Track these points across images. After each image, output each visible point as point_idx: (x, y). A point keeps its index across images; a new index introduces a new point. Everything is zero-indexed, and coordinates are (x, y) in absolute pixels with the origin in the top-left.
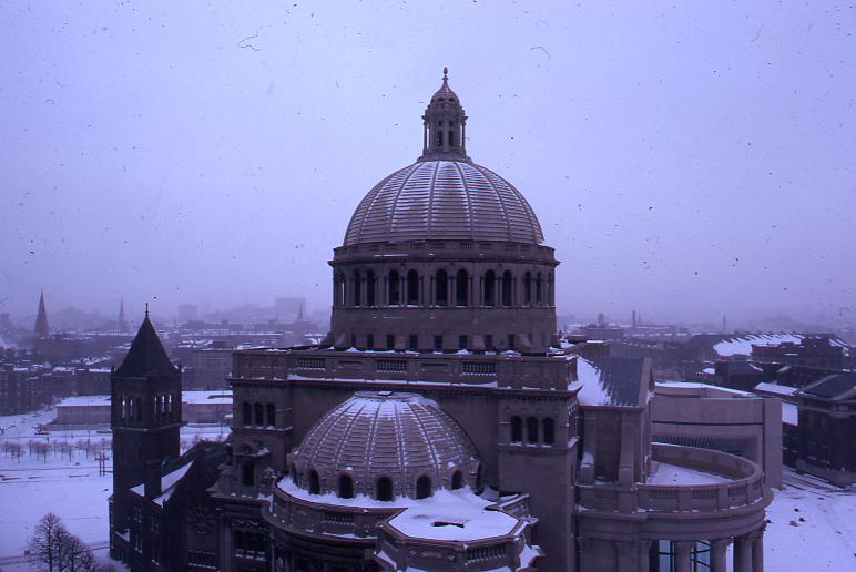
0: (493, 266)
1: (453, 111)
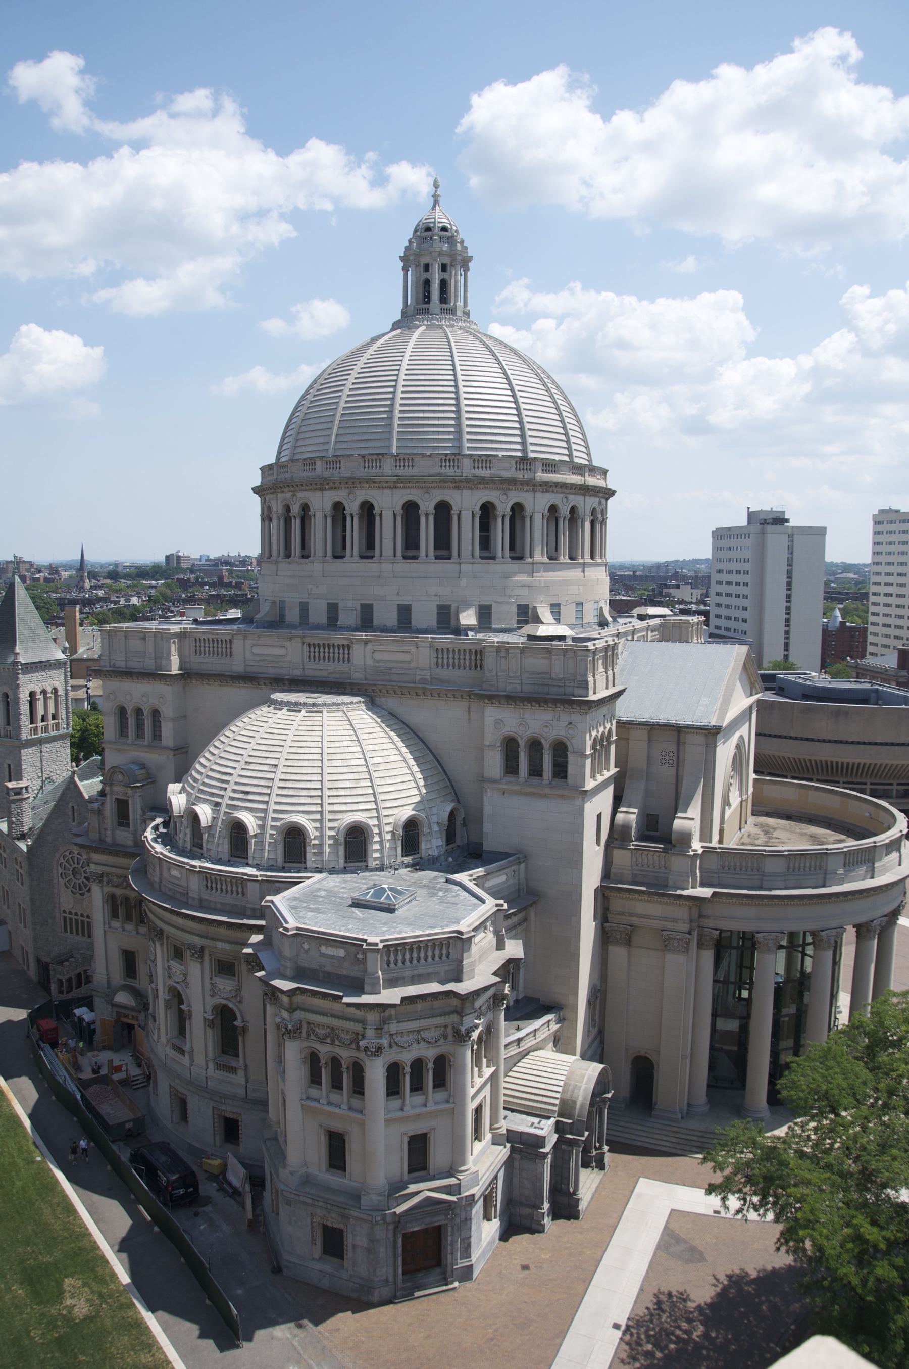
0: (492, 495)
1: (445, 247)
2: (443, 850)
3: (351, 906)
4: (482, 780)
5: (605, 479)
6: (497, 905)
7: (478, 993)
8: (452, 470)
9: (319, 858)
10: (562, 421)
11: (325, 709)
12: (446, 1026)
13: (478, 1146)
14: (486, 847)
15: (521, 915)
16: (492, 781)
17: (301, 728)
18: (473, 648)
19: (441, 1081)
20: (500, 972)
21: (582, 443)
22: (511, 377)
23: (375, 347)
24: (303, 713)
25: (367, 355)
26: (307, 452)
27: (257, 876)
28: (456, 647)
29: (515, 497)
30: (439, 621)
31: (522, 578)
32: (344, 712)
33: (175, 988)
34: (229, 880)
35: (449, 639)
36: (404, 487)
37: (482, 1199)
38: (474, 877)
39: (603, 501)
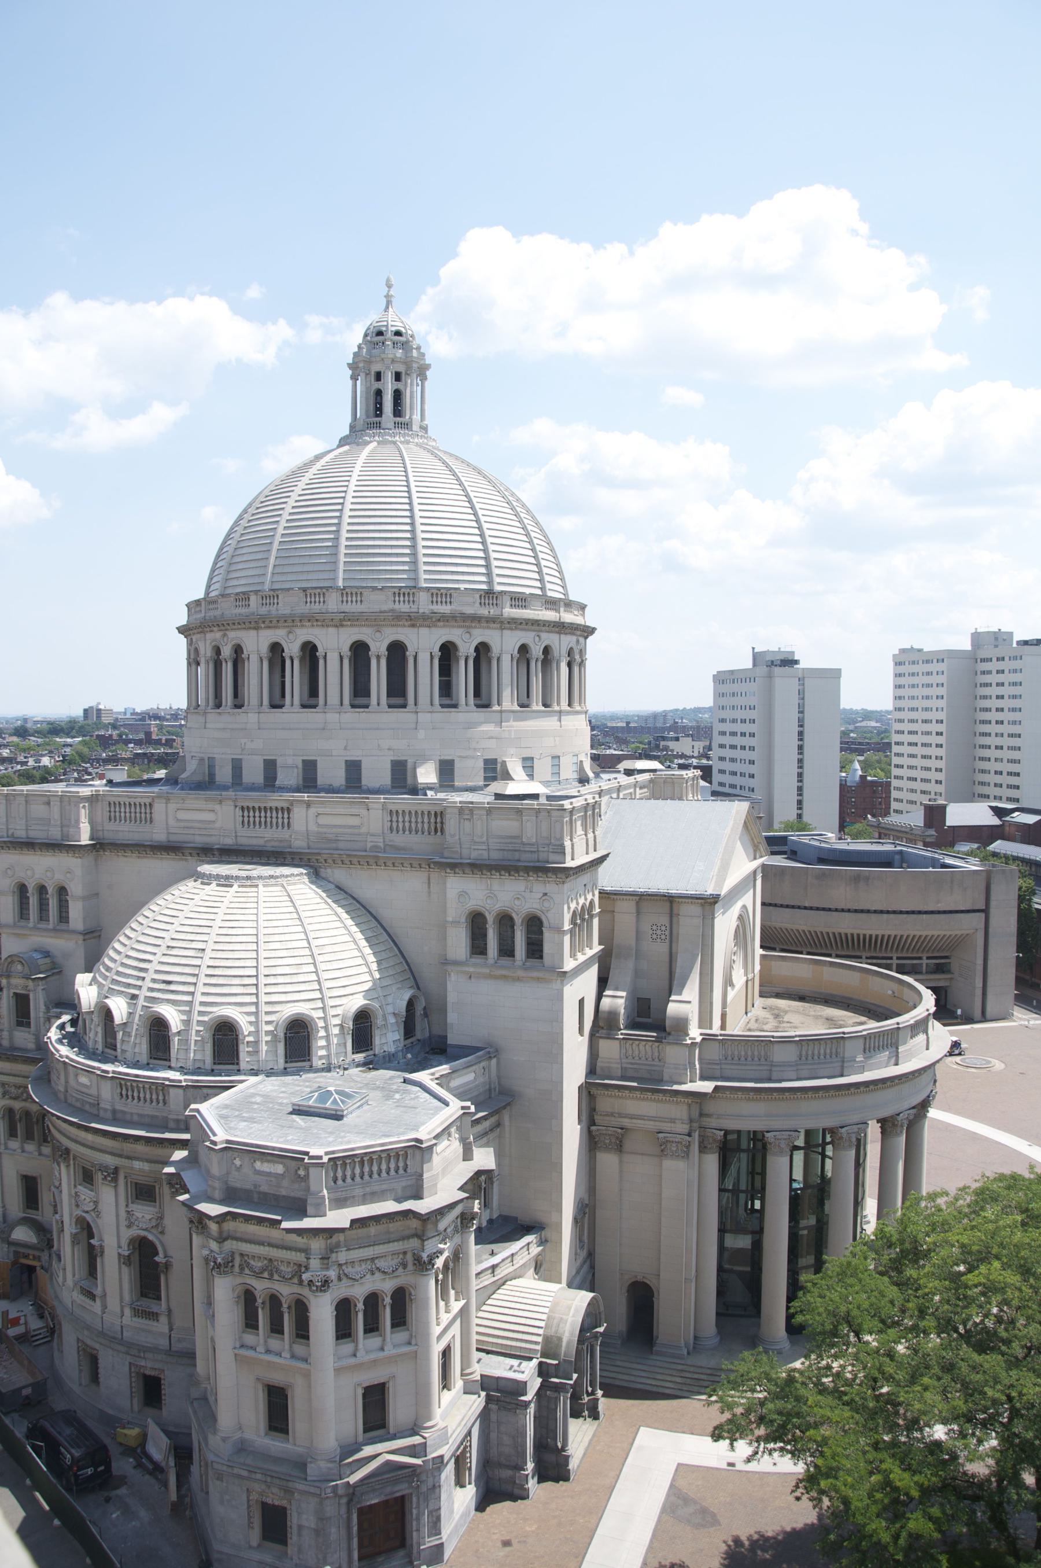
1: (399, 353)
2: (401, 1045)
3: (291, 1113)
4: (446, 962)
5: (583, 615)
6: (463, 1108)
7: (441, 1212)
8: (407, 605)
9: (254, 1058)
10: (533, 550)
11: (260, 883)
12: (405, 1253)
13: (447, 1396)
14: (451, 1041)
15: (493, 1120)
16: (456, 963)
17: (232, 905)
18: (433, 809)
19: (400, 1320)
20: (469, 1187)
21: (557, 574)
22: (475, 500)
23: (319, 465)
24: (235, 887)
25: (309, 475)
26: (239, 585)
27: (180, 1081)
28: (413, 809)
29: (480, 635)
30: (394, 779)
31: (489, 728)
32: (283, 886)
33: (84, 1218)
34: (147, 1086)
35: (403, 801)
36: (351, 626)
37: (453, 1460)
38: (437, 1076)
39: (581, 640)
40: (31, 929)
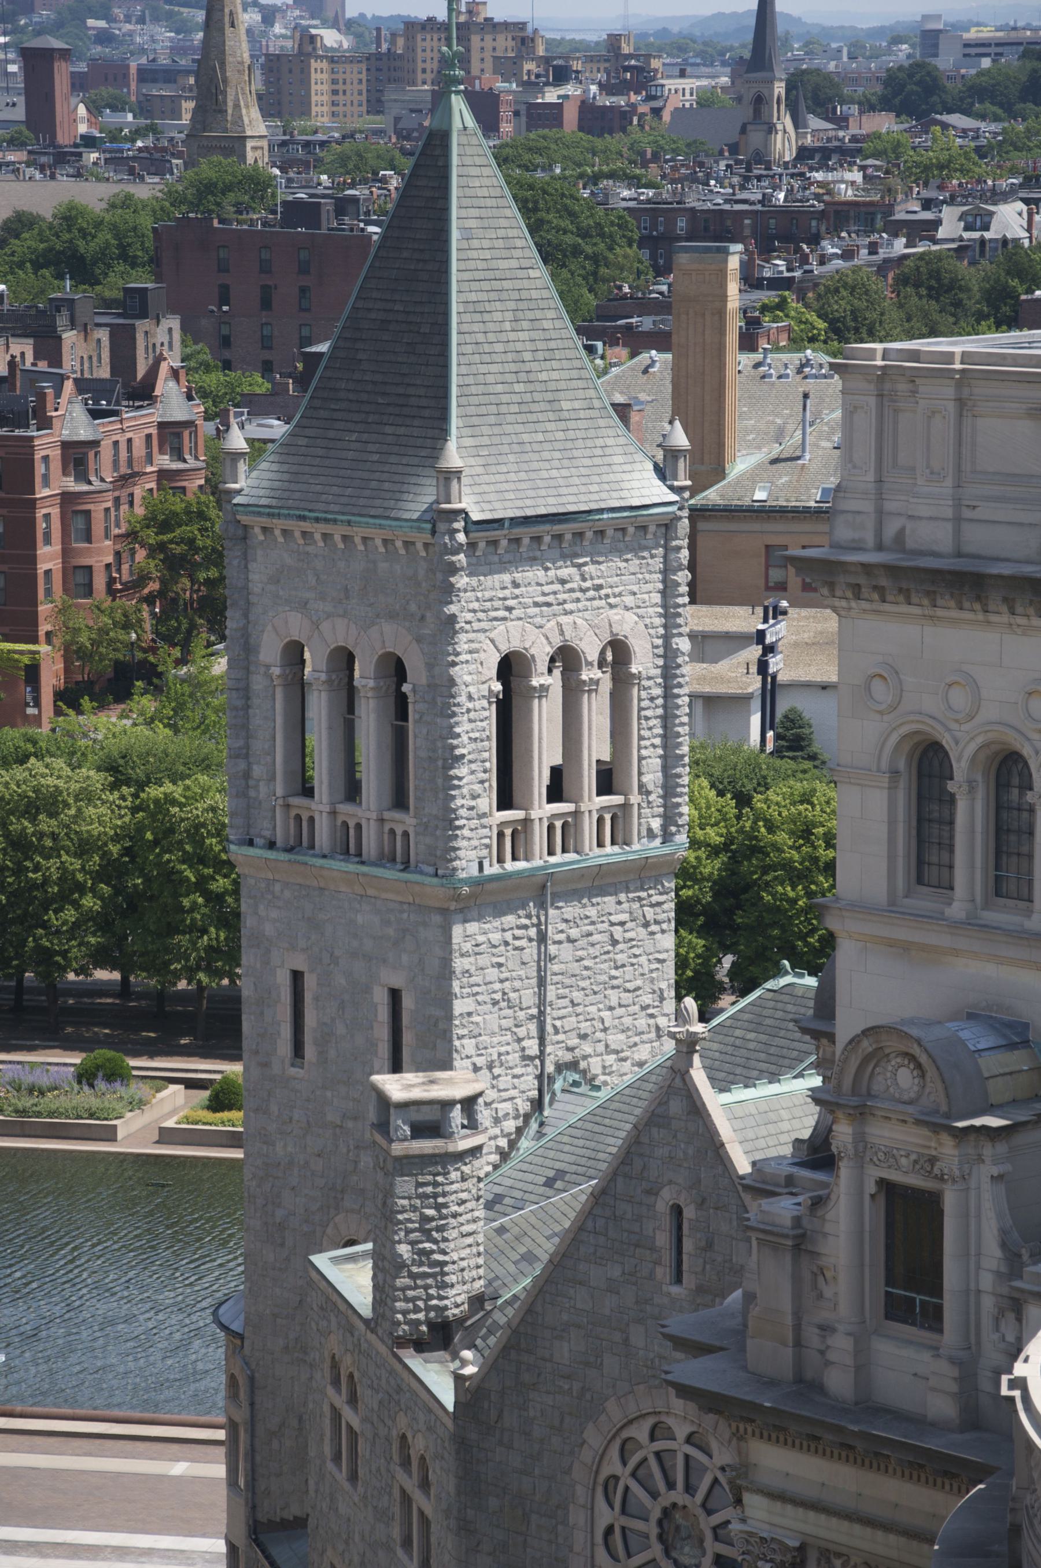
40: (956, 926)
